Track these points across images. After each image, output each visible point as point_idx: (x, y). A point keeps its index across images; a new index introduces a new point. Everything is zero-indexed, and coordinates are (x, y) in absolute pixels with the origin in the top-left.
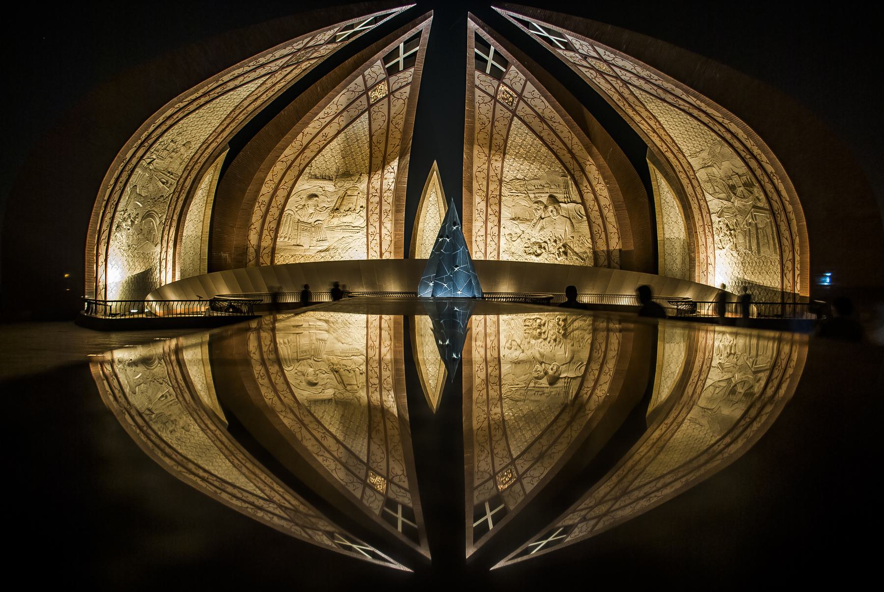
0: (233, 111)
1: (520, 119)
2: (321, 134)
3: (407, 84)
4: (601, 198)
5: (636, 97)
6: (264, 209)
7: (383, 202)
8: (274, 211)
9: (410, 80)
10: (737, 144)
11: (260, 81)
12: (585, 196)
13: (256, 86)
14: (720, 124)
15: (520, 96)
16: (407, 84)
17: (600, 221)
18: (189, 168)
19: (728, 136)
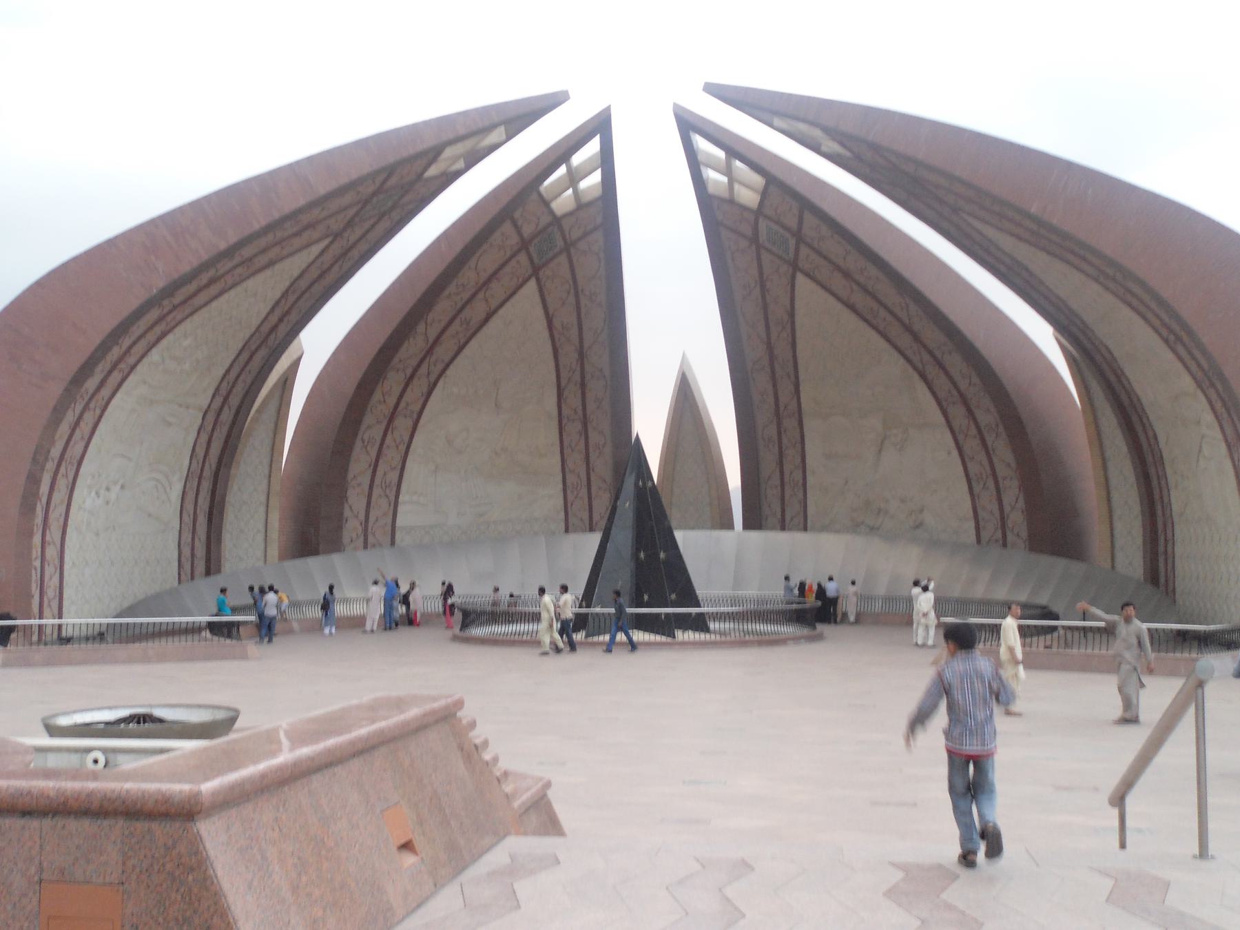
0: (285, 294)
1: (807, 275)
2: (457, 321)
3: (595, 229)
4: (979, 414)
5: (981, 233)
6: (374, 454)
7: (591, 434)
8: (392, 456)
9: (599, 220)
10: (1150, 316)
11: (316, 249)
12: (951, 410)
13: (312, 257)
14: (1114, 280)
15: (798, 235)
16: (595, 229)
17: (982, 457)
18: (223, 392)
19: (1135, 302)
